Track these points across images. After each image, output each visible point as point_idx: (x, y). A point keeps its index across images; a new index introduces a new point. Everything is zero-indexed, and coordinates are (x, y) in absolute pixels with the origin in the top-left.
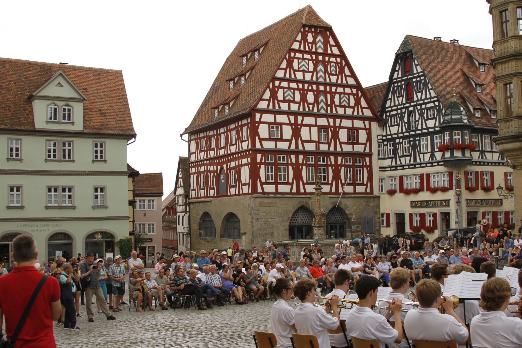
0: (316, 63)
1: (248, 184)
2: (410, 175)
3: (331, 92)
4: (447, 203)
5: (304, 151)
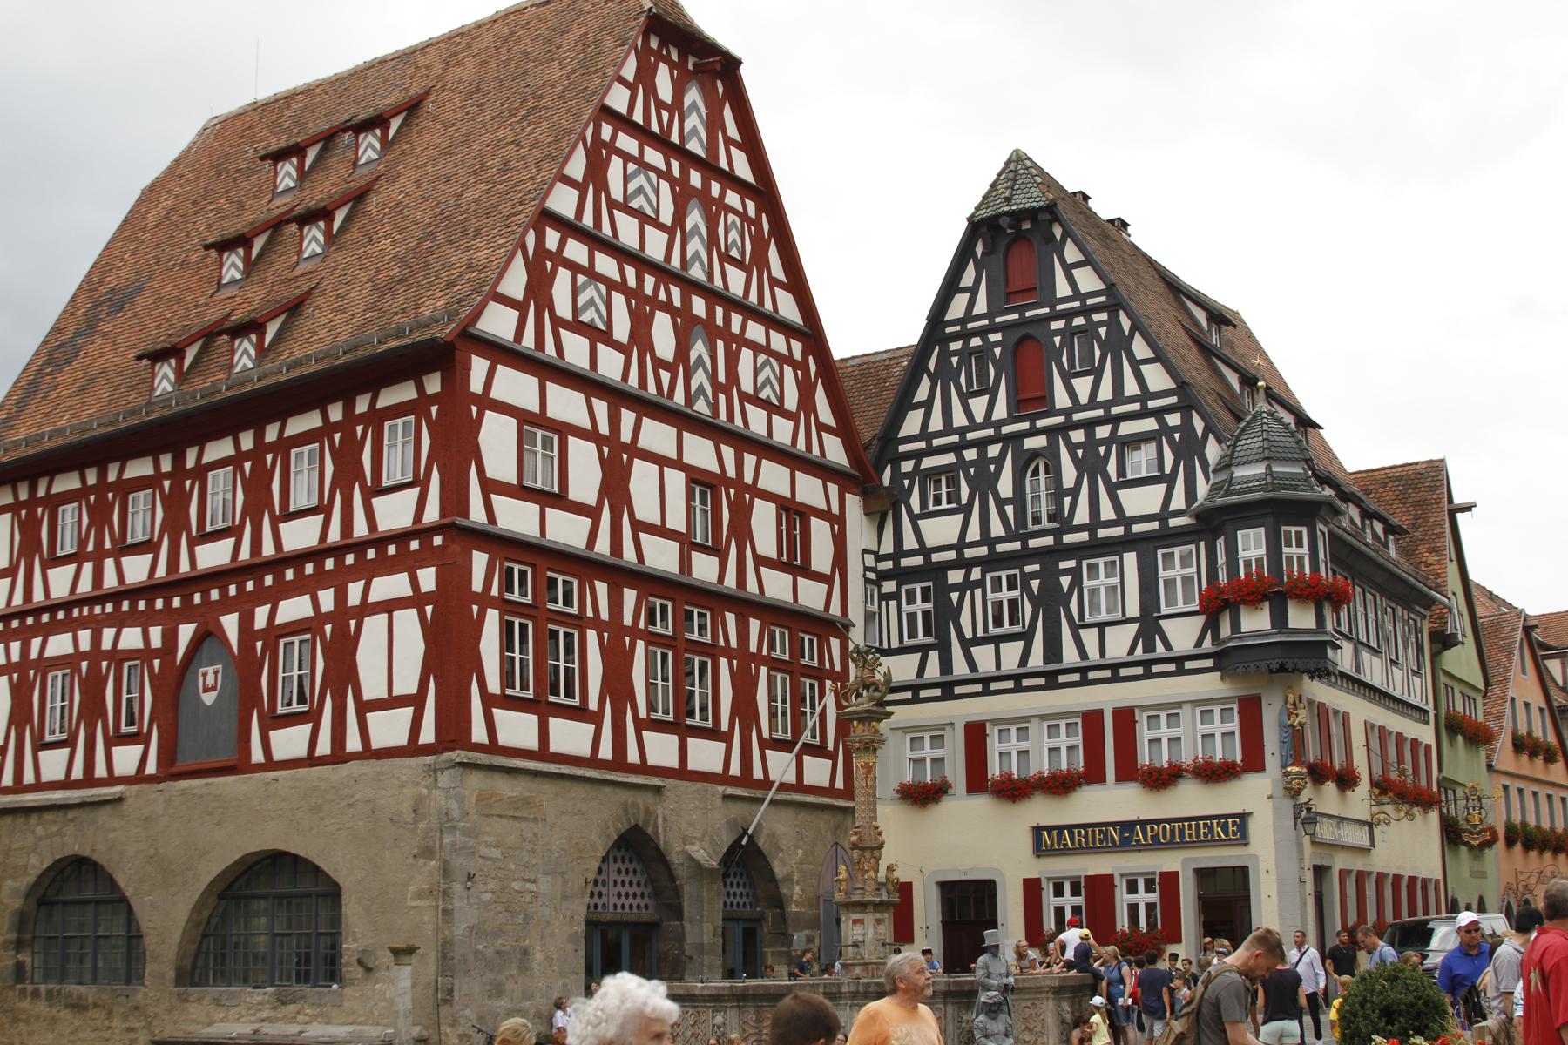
0: (683, 197)
1: (417, 701)
2: (1027, 719)
3: (725, 333)
4: (1237, 826)
5: (640, 568)
